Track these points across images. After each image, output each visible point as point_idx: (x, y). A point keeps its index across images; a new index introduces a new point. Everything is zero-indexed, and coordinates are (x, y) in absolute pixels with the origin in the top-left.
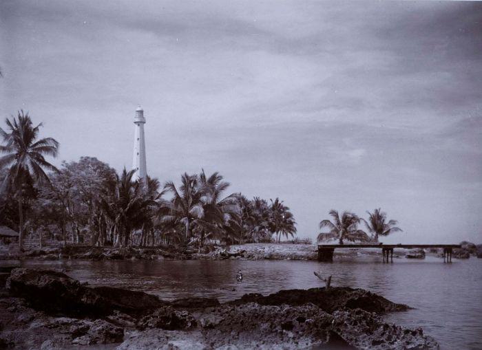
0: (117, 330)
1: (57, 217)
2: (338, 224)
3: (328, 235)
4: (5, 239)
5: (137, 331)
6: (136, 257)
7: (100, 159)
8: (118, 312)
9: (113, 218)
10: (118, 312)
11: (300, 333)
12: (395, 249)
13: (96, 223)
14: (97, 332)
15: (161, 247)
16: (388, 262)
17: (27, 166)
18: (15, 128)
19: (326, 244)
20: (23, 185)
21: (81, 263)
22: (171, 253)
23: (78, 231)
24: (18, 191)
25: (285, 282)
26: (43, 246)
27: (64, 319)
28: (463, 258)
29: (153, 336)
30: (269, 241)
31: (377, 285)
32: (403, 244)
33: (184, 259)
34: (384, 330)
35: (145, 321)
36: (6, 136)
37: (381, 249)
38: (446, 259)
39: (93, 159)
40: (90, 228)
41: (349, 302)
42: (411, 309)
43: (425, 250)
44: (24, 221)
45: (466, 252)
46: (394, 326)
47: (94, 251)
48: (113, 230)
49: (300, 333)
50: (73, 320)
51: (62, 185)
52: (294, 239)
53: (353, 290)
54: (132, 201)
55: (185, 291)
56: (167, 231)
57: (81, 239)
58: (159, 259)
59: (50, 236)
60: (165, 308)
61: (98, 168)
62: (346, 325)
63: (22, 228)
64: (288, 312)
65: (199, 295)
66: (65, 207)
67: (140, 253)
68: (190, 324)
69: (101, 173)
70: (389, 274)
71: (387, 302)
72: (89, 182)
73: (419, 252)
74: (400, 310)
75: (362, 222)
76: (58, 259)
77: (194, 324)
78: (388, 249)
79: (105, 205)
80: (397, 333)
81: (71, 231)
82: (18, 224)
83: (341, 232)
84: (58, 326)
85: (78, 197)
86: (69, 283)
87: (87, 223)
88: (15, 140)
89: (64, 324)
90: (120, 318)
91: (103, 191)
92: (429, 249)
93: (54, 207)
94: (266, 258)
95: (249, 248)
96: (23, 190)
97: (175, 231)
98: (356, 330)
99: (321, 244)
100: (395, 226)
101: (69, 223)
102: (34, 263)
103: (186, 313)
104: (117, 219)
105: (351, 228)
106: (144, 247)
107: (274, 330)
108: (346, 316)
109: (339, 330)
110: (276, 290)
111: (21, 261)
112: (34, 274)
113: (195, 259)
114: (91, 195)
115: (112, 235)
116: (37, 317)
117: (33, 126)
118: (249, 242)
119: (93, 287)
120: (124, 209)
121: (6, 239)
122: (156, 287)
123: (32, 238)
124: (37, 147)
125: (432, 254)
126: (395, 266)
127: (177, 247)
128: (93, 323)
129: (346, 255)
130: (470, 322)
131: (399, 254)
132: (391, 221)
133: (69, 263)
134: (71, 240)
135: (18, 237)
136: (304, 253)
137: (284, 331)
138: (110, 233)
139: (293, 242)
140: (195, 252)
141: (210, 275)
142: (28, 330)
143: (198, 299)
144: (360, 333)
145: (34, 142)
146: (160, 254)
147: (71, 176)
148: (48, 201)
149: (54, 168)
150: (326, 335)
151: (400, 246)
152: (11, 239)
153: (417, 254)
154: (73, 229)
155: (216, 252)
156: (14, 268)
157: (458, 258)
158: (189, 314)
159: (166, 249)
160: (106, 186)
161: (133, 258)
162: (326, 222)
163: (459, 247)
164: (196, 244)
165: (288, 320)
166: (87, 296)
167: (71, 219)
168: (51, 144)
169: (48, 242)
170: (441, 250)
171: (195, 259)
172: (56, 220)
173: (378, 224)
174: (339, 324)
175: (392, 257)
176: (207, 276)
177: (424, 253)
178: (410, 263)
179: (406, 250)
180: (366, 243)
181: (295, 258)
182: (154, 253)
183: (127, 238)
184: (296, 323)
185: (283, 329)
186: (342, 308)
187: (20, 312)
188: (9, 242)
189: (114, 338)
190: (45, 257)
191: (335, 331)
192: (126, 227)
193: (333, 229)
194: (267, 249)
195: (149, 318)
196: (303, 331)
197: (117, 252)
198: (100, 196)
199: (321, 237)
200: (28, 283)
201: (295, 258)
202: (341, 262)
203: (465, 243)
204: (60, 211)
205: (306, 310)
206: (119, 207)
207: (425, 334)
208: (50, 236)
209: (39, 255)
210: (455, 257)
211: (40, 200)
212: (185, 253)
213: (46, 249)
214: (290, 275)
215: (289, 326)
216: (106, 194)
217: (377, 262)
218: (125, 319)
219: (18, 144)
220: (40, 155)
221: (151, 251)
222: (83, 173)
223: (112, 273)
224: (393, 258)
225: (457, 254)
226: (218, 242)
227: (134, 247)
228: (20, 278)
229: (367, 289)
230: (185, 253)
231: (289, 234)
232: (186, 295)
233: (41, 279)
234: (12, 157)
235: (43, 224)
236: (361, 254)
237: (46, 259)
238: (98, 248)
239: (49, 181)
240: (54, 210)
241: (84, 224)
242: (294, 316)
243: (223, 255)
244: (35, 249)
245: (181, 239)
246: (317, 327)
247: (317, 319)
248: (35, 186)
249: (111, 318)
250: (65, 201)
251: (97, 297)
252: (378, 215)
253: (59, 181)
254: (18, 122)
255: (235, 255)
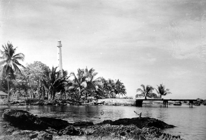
0: (49, 136)
1: (24, 87)
2: (145, 90)
3: (140, 95)
4: (2, 97)
5: (58, 136)
6: (58, 104)
7: (42, 62)
8: (50, 128)
9: (48, 88)
10: (50, 128)
11: (128, 137)
12: (169, 101)
13: (41, 90)
14: (41, 136)
15: (68, 100)
16: (165, 107)
17: (11, 65)
18: (6, 49)
19: (139, 99)
20: (9, 73)
21: (34, 107)
22: (73, 102)
23: (33, 93)
24: (7, 76)
25: (122, 115)
26: (18, 99)
27: (27, 131)
28: (198, 105)
29: (65, 138)
30: (115, 98)
31: (161, 117)
32: (172, 99)
33: (78, 105)
34: (164, 136)
35: (61, 132)
36: (2, 52)
37: (163, 101)
38: (190, 106)
39: (39, 62)
40: (38, 92)
41: (149, 124)
42: (175, 127)
43: (181, 102)
44: (10, 89)
45: (199, 103)
46: (168, 134)
47: (40, 102)
48: (48, 93)
49: (128, 137)
50: (31, 131)
51: (26, 73)
52: (125, 97)
53: (151, 119)
54: (56, 80)
55: (78, 119)
56: (71, 93)
57: (34, 96)
58: (68, 105)
59: (21, 95)
60: (70, 126)
61: (41, 66)
62: (148, 134)
63: (9, 92)
64: (123, 128)
65: (85, 120)
66: (27, 83)
67: (60, 103)
68: (81, 133)
69: (43, 68)
70: (166, 112)
71: (165, 124)
72: (38, 72)
73: (179, 103)
74: (171, 128)
75: (155, 89)
76: (24, 105)
77: (83, 133)
78: (166, 101)
79: (44, 82)
80: (170, 137)
81: (30, 93)
82: (7, 90)
83: (146, 94)
84: (24, 134)
85: (33, 79)
86: (29, 115)
87: (37, 89)
88: (6, 54)
89: (27, 133)
90: (51, 130)
91: (44, 76)
92: (183, 101)
93: (23, 83)
94: (113, 105)
95: (106, 100)
96: (9, 76)
97: (74, 93)
98: (152, 136)
99: (137, 99)
100: (169, 91)
101: (29, 90)
102: (14, 107)
103: (79, 128)
104: (50, 88)
105: (150, 92)
106: (61, 100)
107: (117, 136)
108: (148, 130)
109: (144, 136)
110: (118, 118)
111: (9, 106)
112: (14, 111)
113: (83, 105)
114: (39, 77)
115: (47, 95)
116: (16, 130)
117: (14, 48)
118: (106, 98)
119: (39, 117)
120: (53, 84)
121: (2, 97)
122: (66, 117)
123: (13, 96)
124: (15, 57)
125: (185, 103)
126: (168, 109)
127: (75, 100)
128: (39, 132)
129: (148, 103)
130: (200, 133)
131: (170, 104)
132: (167, 89)
133: (29, 107)
134: (30, 97)
135: (7, 96)
136: (130, 103)
137: (121, 136)
138: (47, 94)
139: (125, 98)
140: (83, 102)
141: (90, 112)
142: (11, 136)
143: (84, 122)
144: (154, 137)
145: (14, 55)
146: (68, 103)
147: (30, 69)
148: (20, 81)
149: (23, 66)
150: (139, 138)
151: (171, 100)
152: (4, 96)
153: (178, 104)
154: (31, 92)
155: (92, 102)
156: (6, 109)
157: (195, 105)
158: (80, 129)
159: (71, 101)
160: (45, 74)
161: (57, 105)
162: (139, 89)
163: (196, 100)
164: (84, 99)
165: (123, 131)
166: (37, 121)
167: (30, 88)
168: (21, 56)
169: (20, 98)
170: (188, 102)
171: (83, 105)
172: (24, 88)
173: (162, 91)
174: (145, 133)
175: (167, 105)
176: (88, 112)
177: (181, 103)
178: (175, 107)
179: (173, 102)
180: (156, 99)
181: (126, 105)
182: (66, 102)
183: (54, 96)
184: (126, 132)
185: (120, 135)
186: (146, 126)
187: (8, 128)
188: (3, 98)
189: (48, 139)
190: (19, 104)
191: (143, 136)
192: (53, 91)
193: (142, 92)
194: (114, 101)
195: (63, 131)
196: (129, 136)
197: (49, 102)
198: (42, 78)
199: (137, 96)
200: (12, 115)
201: (126, 105)
202: (146, 107)
203: (199, 99)
204: (25, 85)
205: (130, 127)
206: (50, 83)
207: (181, 137)
208: (21, 95)
209: (16, 103)
210: (194, 105)
211: (17, 80)
212: (79, 102)
213: (19, 101)
214: (124, 112)
215: (123, 134)
216: (45, 77)
217: (161, 107)
218: (53, 131)
219: (7, 56)
220: (17, 60)
221: (64, 102)
222: (35, 68)
223: (47, 111)
224: (168, 105)
225: (195, 103)
226: (93, 98)
227: (57, 100)
228: (8, 113)
229: (157, 118)
230: (79, 102)
231: (123, 95)
232: (79, 121)
233: (17, 114)
234: (5, 61)
235: (18, 90)
236: (154, 103)
237: (19, 105)
238: (41, 100)
239: (20, 71)
240: (23, 84)
241: (36, 90)
242: (126, 130)
243: (95, 103)
244: (15, 101)
245: (77, 97)
246: (135, 134)
247: (135, 131)
248: (15, 74)
249: (47, 130)
250: (27, 80)
251: (41, 122)
252: (162, 86)
253: (25, 71)
254: (7, 46)
255: (100, 104)
